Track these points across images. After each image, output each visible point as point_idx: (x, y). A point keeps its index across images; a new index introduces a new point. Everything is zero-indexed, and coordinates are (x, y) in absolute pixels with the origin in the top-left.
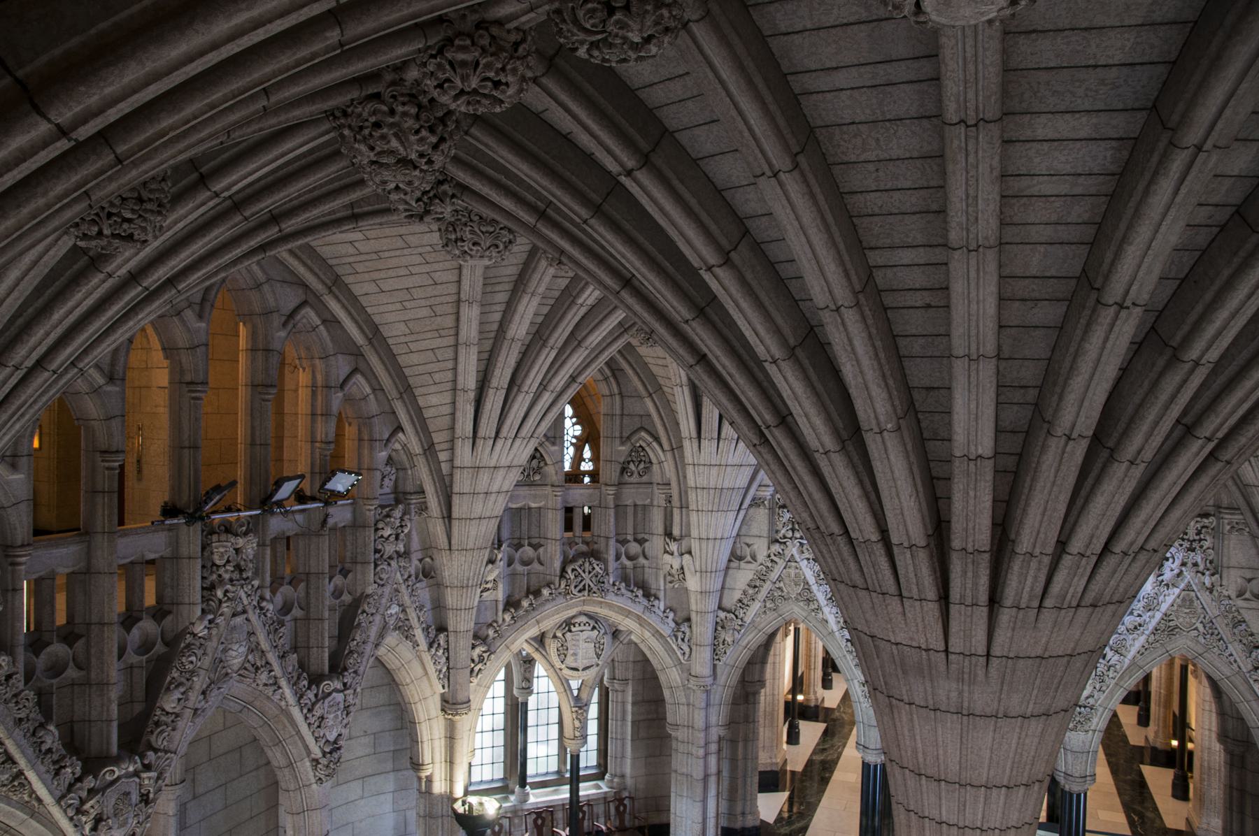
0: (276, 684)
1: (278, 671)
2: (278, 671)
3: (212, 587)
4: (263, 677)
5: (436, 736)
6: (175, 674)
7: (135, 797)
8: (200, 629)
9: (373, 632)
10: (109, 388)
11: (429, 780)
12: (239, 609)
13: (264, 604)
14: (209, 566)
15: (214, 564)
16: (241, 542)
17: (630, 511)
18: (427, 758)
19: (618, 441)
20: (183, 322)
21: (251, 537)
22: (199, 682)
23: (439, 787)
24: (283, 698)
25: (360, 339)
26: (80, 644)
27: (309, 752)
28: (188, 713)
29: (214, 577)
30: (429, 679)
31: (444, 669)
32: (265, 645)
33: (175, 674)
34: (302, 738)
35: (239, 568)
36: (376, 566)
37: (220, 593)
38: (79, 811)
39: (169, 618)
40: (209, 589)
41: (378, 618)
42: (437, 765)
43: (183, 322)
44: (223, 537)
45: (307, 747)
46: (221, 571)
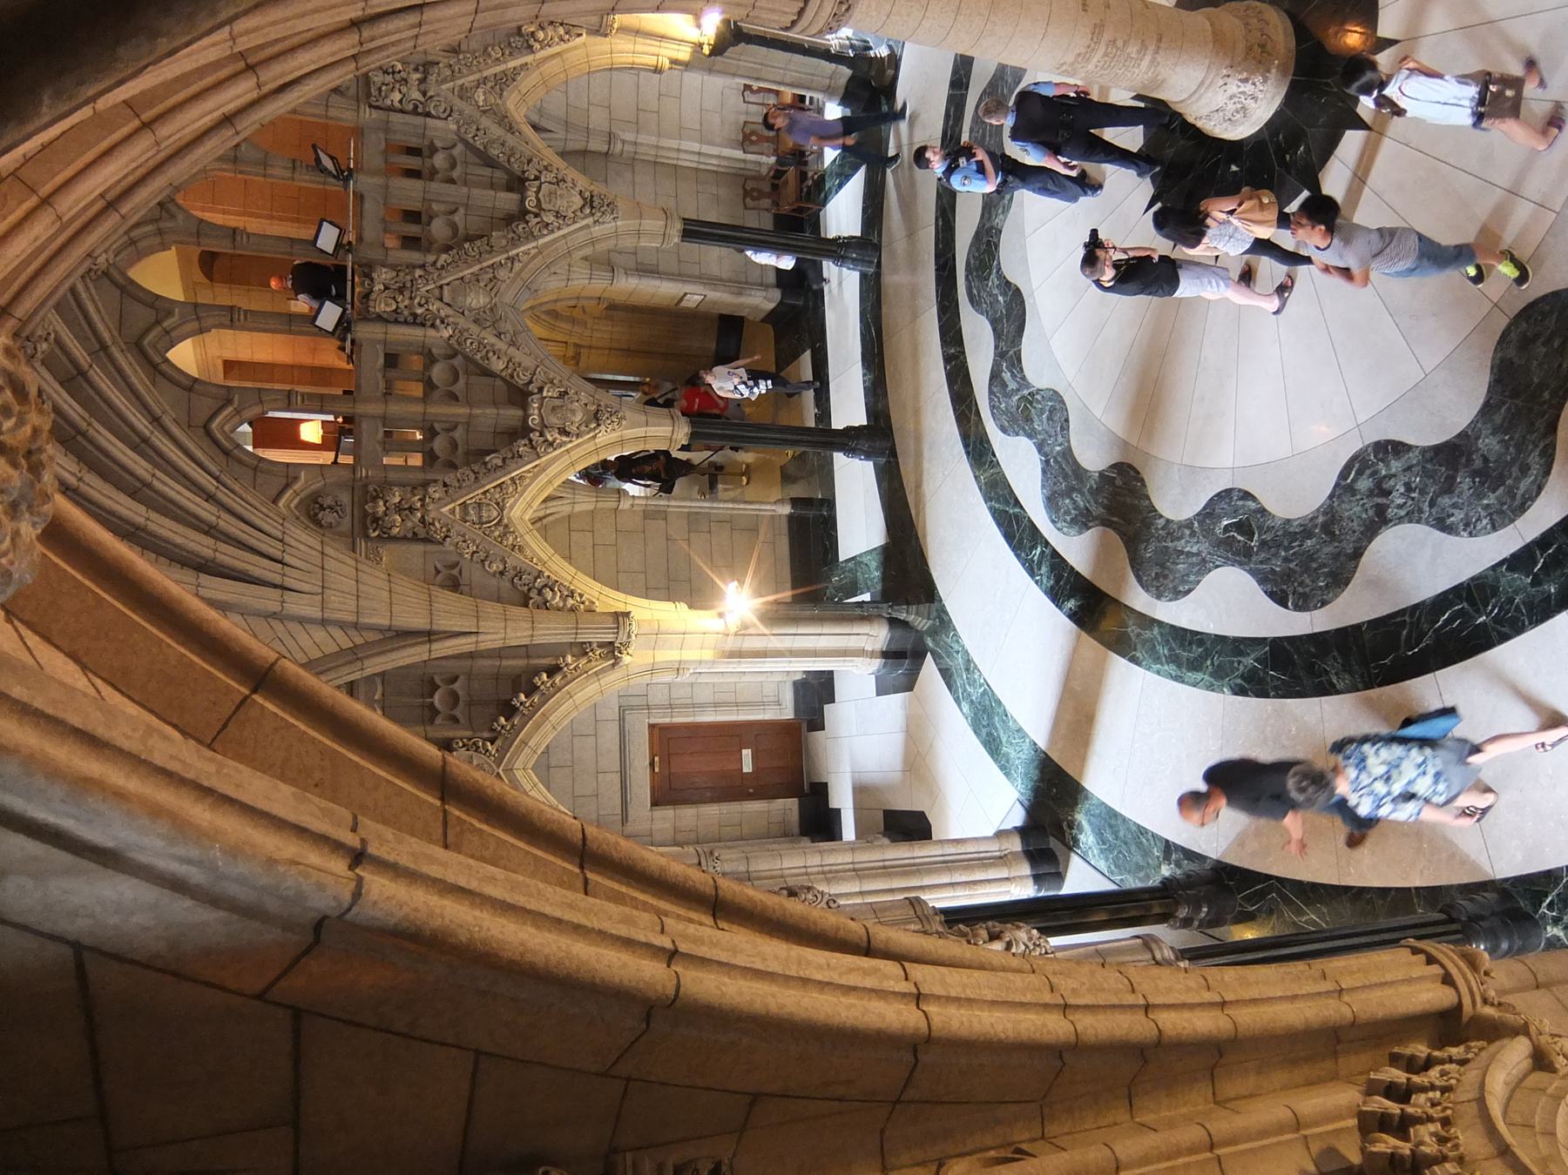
0: (512, 260)
1: (502, 258)
2: (502, 258)
3: (415, 316)
4: (502, 274)
5: (631, 47)
6: (478, 356)
7: (558, 402)
8: (446, 333)
9: (496, 131)
11: (674, 62)
12: (437, 292)
13: (439, 265)
14: (395, 319)
15: (395, 311)
16: (378, 287)
18: (652, 61)
20: (174, 329)
21: (375, 275)
22: (489, 338)
23: (684, 54)
24: (526, 253)
26: (437, 426)
27: (587, 226)
28: (512, 350)
29: (406, 313)
30: (566, 51)
31: (561, 31)
32: (476, 268)
33: (478, 356)
34: (570, 234)
35: (401, 290)
36: (428, 115)
37: (419, 311)
38: (551, 444)
39: (434, 351)
40: (416, 321)
41: (485, 122)
42: (663, 51)
43: (174, 329)
44: (371, 303)
45: (581, 229)
46: (402, 306)
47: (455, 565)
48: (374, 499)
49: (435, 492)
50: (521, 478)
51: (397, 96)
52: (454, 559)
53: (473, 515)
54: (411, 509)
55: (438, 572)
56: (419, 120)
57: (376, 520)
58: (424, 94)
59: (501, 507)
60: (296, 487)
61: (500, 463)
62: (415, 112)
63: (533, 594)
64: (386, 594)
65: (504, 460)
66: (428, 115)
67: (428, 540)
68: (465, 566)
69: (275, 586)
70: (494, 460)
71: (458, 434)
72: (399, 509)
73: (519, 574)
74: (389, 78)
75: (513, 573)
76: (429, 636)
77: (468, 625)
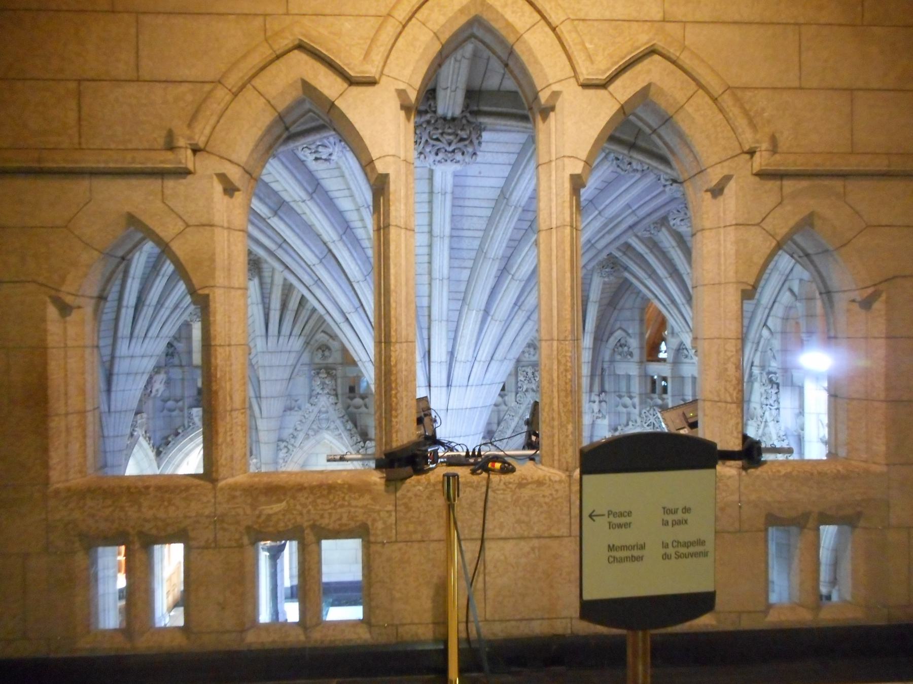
17: (690, 380)
36: (517, 393)
47: (300, 408)
48: (328, 373)
49: (332, 399)
50: (342, 438)
51: (523, 379)
52: (303, 408)
53: (323, 416)
54: (322, 389)
55: (296, 401)
56: (514, 389)
57: (318, 373)
58: (527, 391)
59: (328, 428)
60: (331, 341)
61: (348, 427)
62: (517, 387)
63: (285, 444)
64: (274, 378)
65: (350, 430)
66: (517, 393)
67: (310, 397)
68: (300, 413)
69: (279, 332)
70: (350, 425)
71: (363, 409)
72: (323, 383)
73: (294, 437)
74: (530, 375)
75: (295, 434)
76: (258, 397)
77: (265, 414)
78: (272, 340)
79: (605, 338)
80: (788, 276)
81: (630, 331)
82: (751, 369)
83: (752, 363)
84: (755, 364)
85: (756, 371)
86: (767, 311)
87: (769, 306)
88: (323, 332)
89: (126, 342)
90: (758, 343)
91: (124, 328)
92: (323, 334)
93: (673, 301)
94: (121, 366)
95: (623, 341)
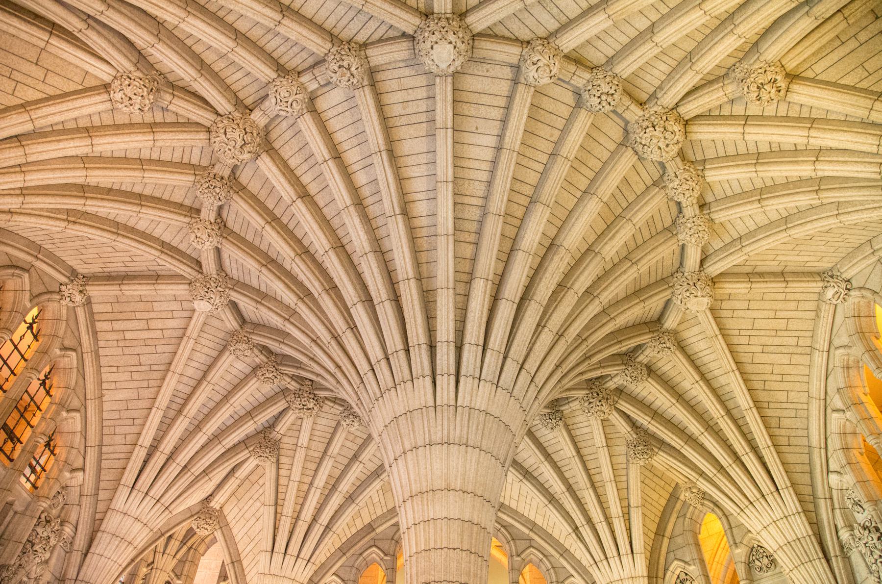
10: (386, 558)
19: (733, 547)
25: (527, 531)
78: (278, 557)
79: (661, 574)
80: (825, 399)
81: (687, 559)
82: (838, 538)
83: (836, 526)
84: (839, 527)
85: (845, 535)
86: (823, 451)
87: (823, 445)
88: (334, 574)
89: (126, 491)
90: (831, 498)
91: (129, 477)
92: (334, 577)
93: (721, 469)
94: (112, 522)
95: (683, 576)
